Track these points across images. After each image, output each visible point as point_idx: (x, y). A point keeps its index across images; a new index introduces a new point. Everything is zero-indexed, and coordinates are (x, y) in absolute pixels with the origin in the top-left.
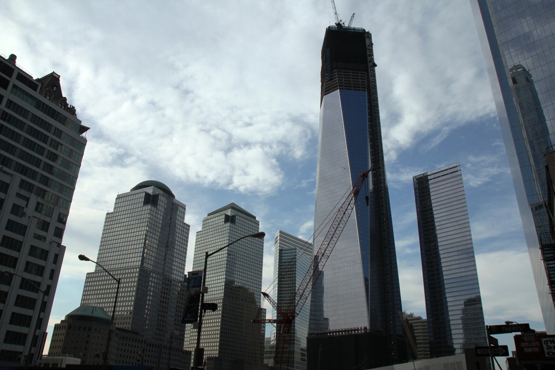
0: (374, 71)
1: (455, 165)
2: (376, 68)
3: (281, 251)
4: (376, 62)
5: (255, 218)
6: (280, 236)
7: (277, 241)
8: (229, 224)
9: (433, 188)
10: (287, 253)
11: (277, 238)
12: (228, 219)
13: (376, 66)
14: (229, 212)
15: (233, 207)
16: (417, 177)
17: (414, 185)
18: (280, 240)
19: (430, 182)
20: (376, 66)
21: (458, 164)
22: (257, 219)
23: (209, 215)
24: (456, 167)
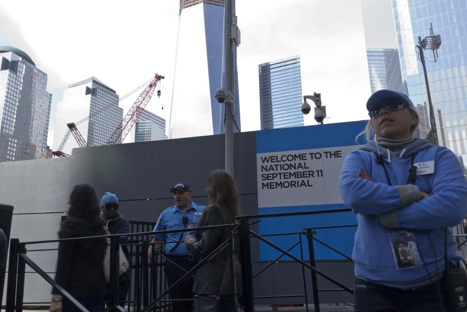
5: (115, 92)
9: (274, 77)
12: (88, 91)
14: (90, 85)
16: (262, 65)
17: (259, 72)
19: (272, 71)
21: (298, 57)
22: (117, 93)
24: (296, 59)
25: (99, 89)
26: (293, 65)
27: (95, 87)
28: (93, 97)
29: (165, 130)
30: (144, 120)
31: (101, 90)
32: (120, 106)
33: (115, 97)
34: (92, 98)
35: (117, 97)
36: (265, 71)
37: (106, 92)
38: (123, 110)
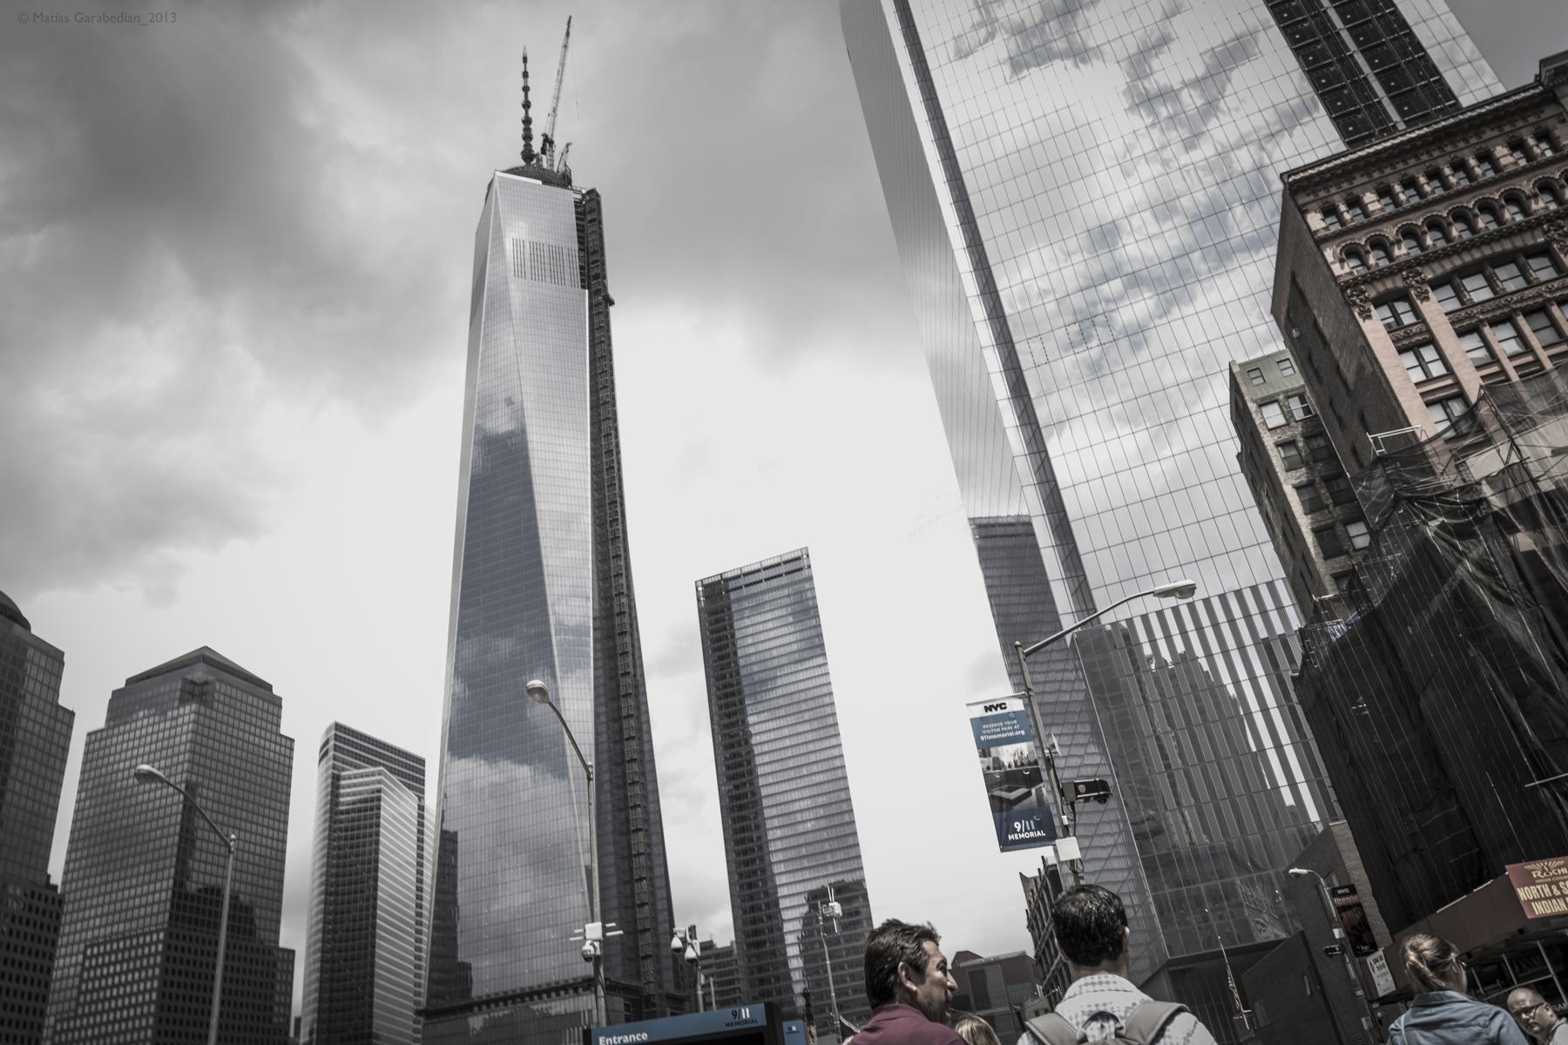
0: (607, 315)
1: (797, 554)
2: (611, 309)
3: (336, 778)
4: (612, 293)
5: (269, 687)
6: (337, 738)
7: (326, 753)
8: (194, 706)
10: (355, 785)
11: (327, 742)
13: (612, 303)
15: (204, 657)
18: (336, 748)
20: (612, 303)
22: (275, 692)
23: (130, 682)
24: (798, 559)
25: (221, 681)
26: (792, 573)
27: (211, 678)
28: (203, 709)
29: (423, 792)
30: (357, 767)
31: (227, 684)
32: (283, 731)
33: (270, 702)
34: (198, 713)
35: (277, 703)
36: (719, 603)
37: (244, 691)
38: (292, 740)
